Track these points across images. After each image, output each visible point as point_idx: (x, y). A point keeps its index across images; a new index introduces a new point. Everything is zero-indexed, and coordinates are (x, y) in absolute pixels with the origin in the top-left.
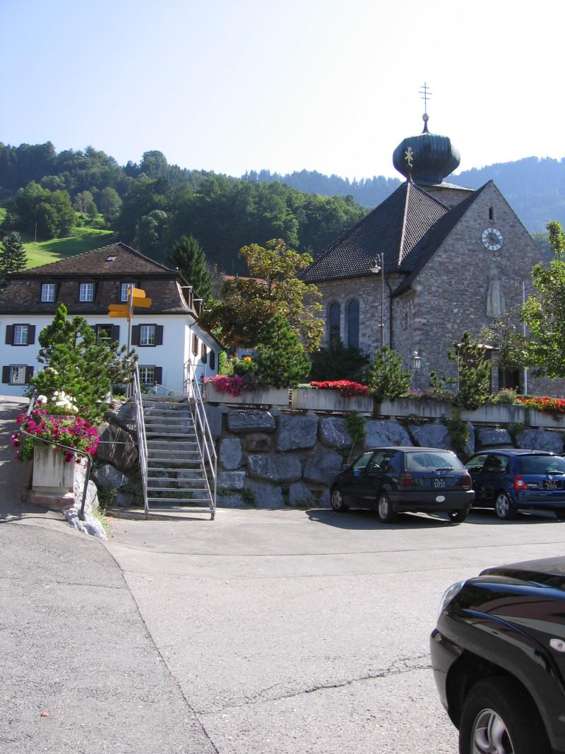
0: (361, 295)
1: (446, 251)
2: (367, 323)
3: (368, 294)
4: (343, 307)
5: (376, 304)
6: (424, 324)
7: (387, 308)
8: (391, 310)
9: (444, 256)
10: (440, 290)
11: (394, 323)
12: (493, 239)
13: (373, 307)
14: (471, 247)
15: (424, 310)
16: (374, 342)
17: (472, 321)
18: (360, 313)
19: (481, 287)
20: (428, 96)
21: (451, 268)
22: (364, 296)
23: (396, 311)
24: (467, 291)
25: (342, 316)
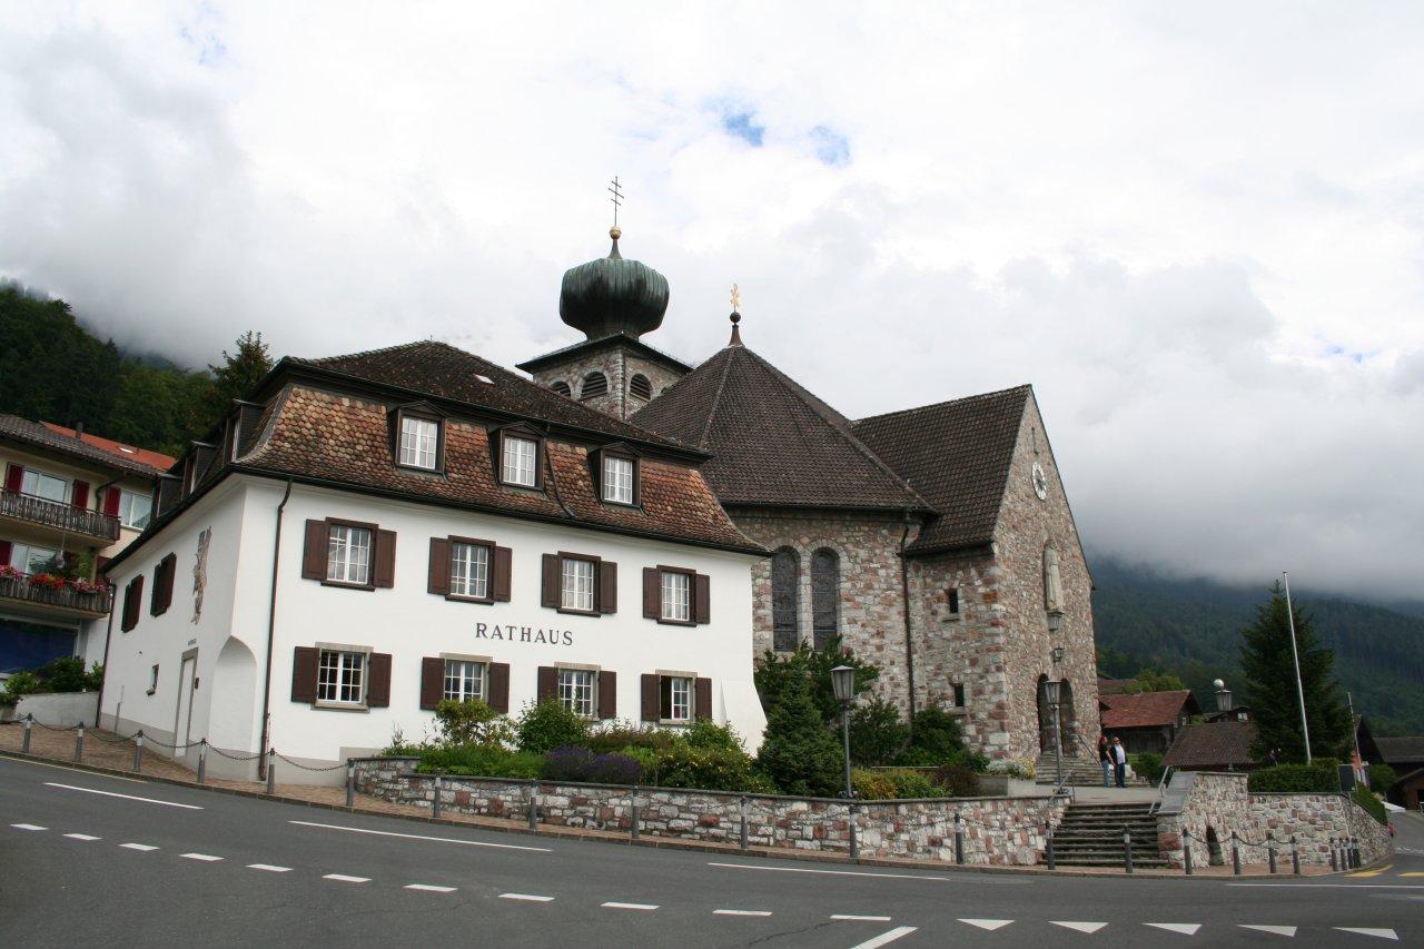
0: (843, 544)
2: (859, 599)
3: (857, 544)
4: (805, 563)
8: (905, 579)
11: (911, 603)
16: (873, 636)
18: (843, 579)
20: (619, 199)
25: (805, 579)
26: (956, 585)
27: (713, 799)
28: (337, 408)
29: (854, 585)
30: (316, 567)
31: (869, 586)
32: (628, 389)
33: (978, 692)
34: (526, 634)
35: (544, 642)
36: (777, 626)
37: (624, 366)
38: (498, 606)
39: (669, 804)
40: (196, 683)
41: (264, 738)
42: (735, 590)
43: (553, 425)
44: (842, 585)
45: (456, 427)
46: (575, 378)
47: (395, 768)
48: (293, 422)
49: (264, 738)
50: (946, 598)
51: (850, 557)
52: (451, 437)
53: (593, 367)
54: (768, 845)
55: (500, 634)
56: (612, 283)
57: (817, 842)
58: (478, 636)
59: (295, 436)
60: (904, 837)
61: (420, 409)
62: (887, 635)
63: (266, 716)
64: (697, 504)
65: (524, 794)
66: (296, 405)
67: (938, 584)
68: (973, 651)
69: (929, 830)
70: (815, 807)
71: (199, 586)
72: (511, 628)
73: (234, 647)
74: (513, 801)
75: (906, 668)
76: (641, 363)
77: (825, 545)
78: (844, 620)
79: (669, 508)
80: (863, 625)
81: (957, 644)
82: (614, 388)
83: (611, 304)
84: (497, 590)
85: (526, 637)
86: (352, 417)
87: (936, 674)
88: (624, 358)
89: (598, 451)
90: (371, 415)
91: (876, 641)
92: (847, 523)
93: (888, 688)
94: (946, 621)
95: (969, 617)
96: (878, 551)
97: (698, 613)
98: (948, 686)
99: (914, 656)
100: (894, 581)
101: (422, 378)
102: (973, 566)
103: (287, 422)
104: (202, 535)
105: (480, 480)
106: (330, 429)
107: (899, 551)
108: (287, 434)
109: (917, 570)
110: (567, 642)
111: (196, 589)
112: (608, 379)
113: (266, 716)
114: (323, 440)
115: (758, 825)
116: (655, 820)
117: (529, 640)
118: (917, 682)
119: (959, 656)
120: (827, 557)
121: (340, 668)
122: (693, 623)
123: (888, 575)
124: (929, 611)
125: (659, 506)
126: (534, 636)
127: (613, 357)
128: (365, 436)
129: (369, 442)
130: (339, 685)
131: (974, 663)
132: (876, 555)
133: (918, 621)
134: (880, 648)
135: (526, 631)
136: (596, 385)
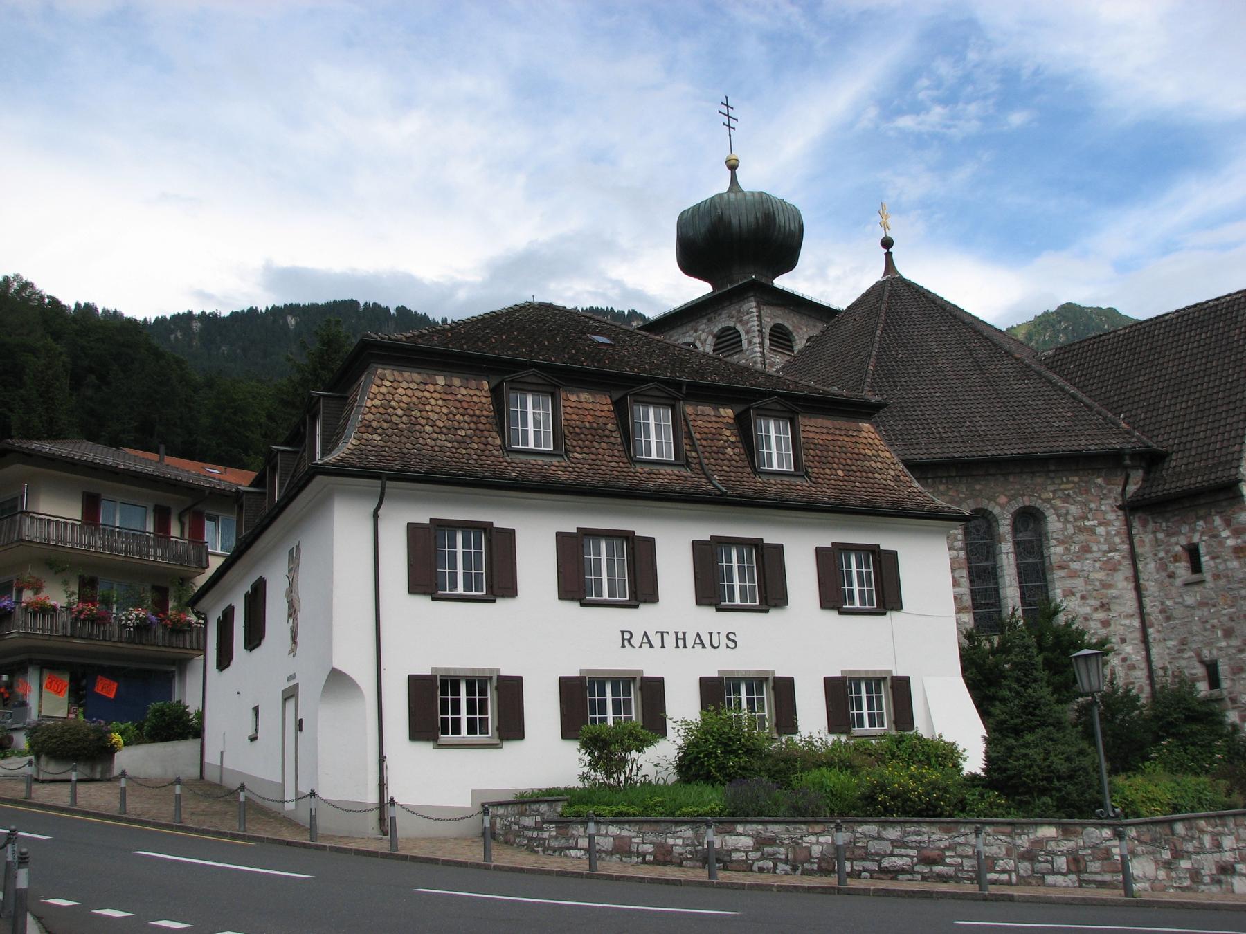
0: (1049, 501)
2: (1075, 566)
3: (1066, 499)
4: (1005, 527)
5: (1091, 523)
7: (1118, 534)
8: (1130, 537)
11: (1140, 566)
16: (1096, 609)
18: (1053, 542)
23: (1142, 541)
26: (1196, 539)
27: (934, 829)
28: (431, 388)
29: (1066, 549)
30: (426, 579)
31: (1086, 549)
32: (767, 342)
34: (681, 640)
35: (704, 647)
36: (975, 606)
37: (759, 316)
38: (645, 609)
39: (880, 838)
40: (300, 725)
41: (382, 785)
43: (689, 385)
44: (1053, 550)
45: (573, 398)
46: (703, 336)
47: (538, 812)
48: (381, 410)
49: (382, 785)
50: (1185, 556)
51: (1059, 516)
52: (569, 410)
53: (723, 321)
54: (1009, 883)
55: (649, 642)
56: (735, 221)
57: (1073, 877)
58: (623, 646)
59: (385, 425)
60: (1185, 864)
61: (529, 380)
62: (1112, 606)
63: (382, 759)
64: (873, 464)
65: (697, 836)
66: (383, 390)
67: (1174, 540)
68: (1226, 618)
69: (1217, 856)
70: (1067, 832)
71: (292, 613)
72: (662, 633)
73: (338, 681)
74: (685, 845)
75: (1142, 646)
76: (779, 312)
77: (1027, 504)
78: (1059, 592)
79: (840, 473)
80: (1083, 598)
81: (1205, 612)
82: (750, 342)
83: (738, 245)
84: (643, 590)
85: (681, 643)
86: (450, 397)
87: (1181, 651)
88: (758, 307)
89: (747, 411)
90: (472, 393)
91: (1101, 615)
92: (1052, 475)
93: (1120, 672)
94: (1186, 585)
95: (1216, 577)
96: (1093, 506)
97: (887, 597)
98: (1198, 665)
99: (1151, 630)
100: (1117, 540)
101: (525, 347)
102: (1217, 513)
103: (374, 410)
104: (291, 552)
105: (609, 459)
106: (424, 414)
107: (1120, 503)
108: (375, 424)
109: (1145, 524)
110: (732, 645)
111: (290, 616)
112: (743, 334)
113: (382, 759)
114: (418, 427)
115: (994, 859)
116: (864, 859)
117: (685, 647)
119: (1208, 626)
120: (1029, 518)
121: (463, 697)
122: (882, 611)
123: (1108, 533)
124: (1164, 574)
125: (827, 471)
126: (690, 640)
127: (745, 307)
128: (467, 418)
129: (472, 425)
130: (464, 716)
131: (1228, 633)
132: (1091, 510)
133: (1151, 587)
134: (1106, 623)
135: (681, 636)
136: (729, 340)
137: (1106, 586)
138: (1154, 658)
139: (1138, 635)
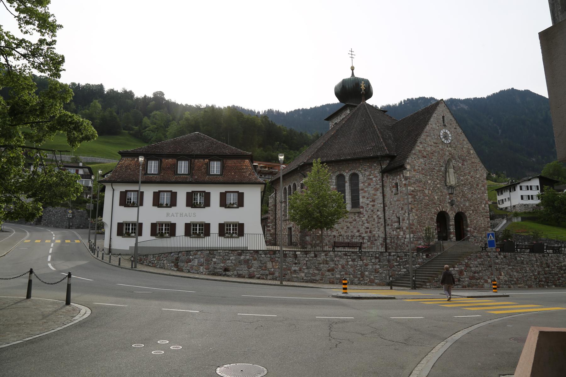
1: (421, 143)
4: (347, 178)
6: (413, 191)
8: (383, 181)
9: (421, 146)
10: (420, 168)
11: (385, 189)
12: (446, 136)
13: (369, 179)
14: (435, 141)
15: (412, 181)
17: (438, 188)
18: (360, 183)
19: (442, 166)
21: (425, 154)
22: (362, 171)
24: (434, 169)
25: (347, 185)
31: (369, 184)
33: (404, 220)
34: (181, 215)
38: (173, 208)
42: (253, 196)
80: (367, 198)
91: (372, 203)
95: (401, 192)
97: (240, 203)
109: (387, 177)
118: (387, 217)
120: (354, 177)
126: (184, 215)
137: (375, 195)
138: (386, 216)
139: (382, 209)
